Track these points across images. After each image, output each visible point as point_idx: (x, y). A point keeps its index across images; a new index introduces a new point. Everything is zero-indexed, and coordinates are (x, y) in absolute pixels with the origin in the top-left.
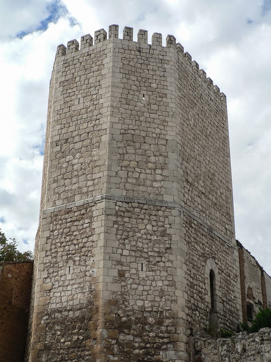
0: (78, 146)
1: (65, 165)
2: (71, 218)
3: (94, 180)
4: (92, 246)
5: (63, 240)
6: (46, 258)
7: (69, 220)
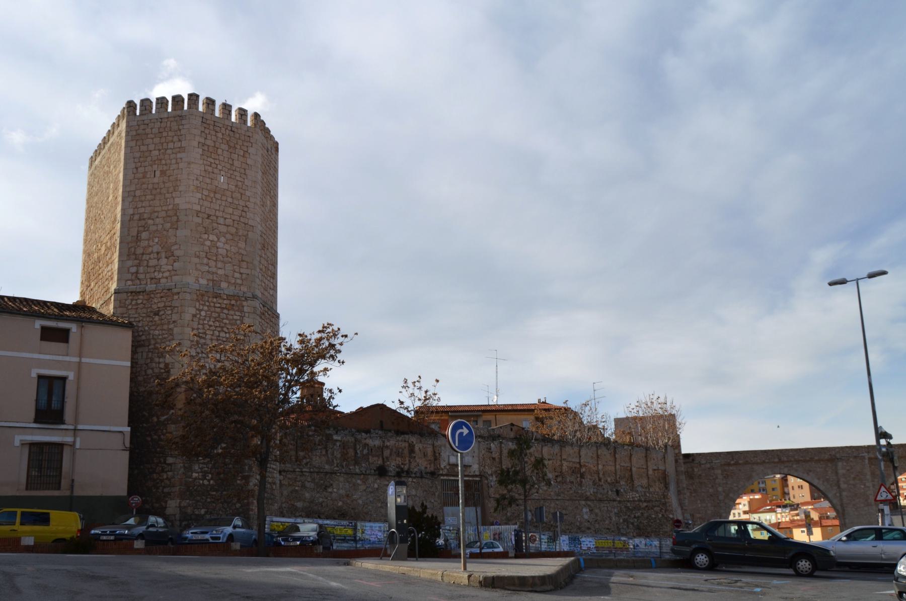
0: (223, 229)
1: (208, 243)
2: (219, 303)
3: (241, 274)
5: (211, 323)
7: (219, 305)
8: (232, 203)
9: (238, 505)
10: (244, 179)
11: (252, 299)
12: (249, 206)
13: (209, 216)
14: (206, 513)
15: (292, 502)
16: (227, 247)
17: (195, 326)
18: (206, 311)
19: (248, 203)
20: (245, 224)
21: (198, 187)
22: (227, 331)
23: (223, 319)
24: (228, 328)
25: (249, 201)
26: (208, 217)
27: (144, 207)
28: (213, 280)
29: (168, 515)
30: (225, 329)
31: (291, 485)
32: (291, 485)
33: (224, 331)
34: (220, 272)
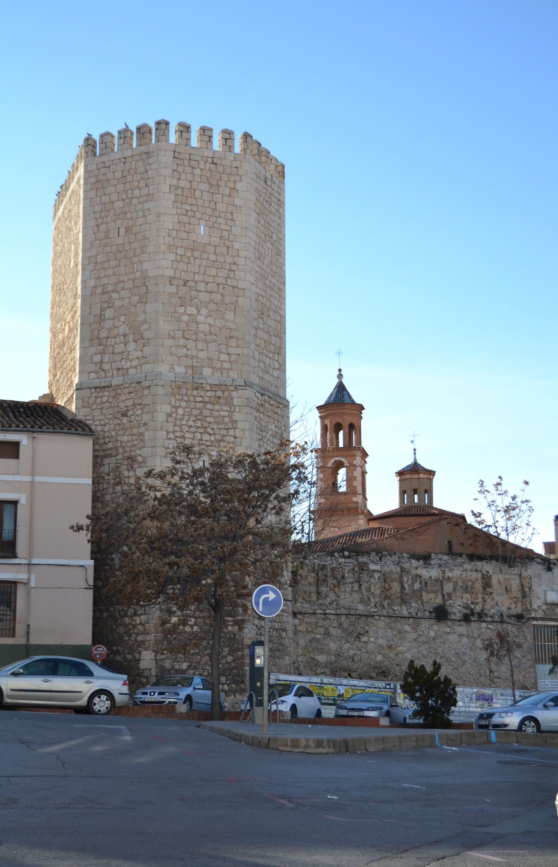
0: (204, 297)
1: (185, 318)
2: (201, 396)
3: (229, 354)
4: (234, 443)
5: (191, 423)
6: (167, 442)
8: (216, 261)
9: (230, 659)
10: (231, 227)
11: (244, 388)
12: (238, 263)
13: (186, 282)
14: (189, 667)
15: (312, 655)
16: (210, 320)
17: (171, 429)
18: (184, 408)
19: (238, 258)
20: (234, 287)
21: (170, 245)
22: (211, 432)
23: (206, 417)
24: (212, 429)
25: (238, 256)
26: (185, 283)
27: (108, 277)
28: (193, 367)
29: (143, 670)
30: (209, 430)
31: (310, 632)
32: (310, 632)
33: (207, 433)
34: (202, 355)
